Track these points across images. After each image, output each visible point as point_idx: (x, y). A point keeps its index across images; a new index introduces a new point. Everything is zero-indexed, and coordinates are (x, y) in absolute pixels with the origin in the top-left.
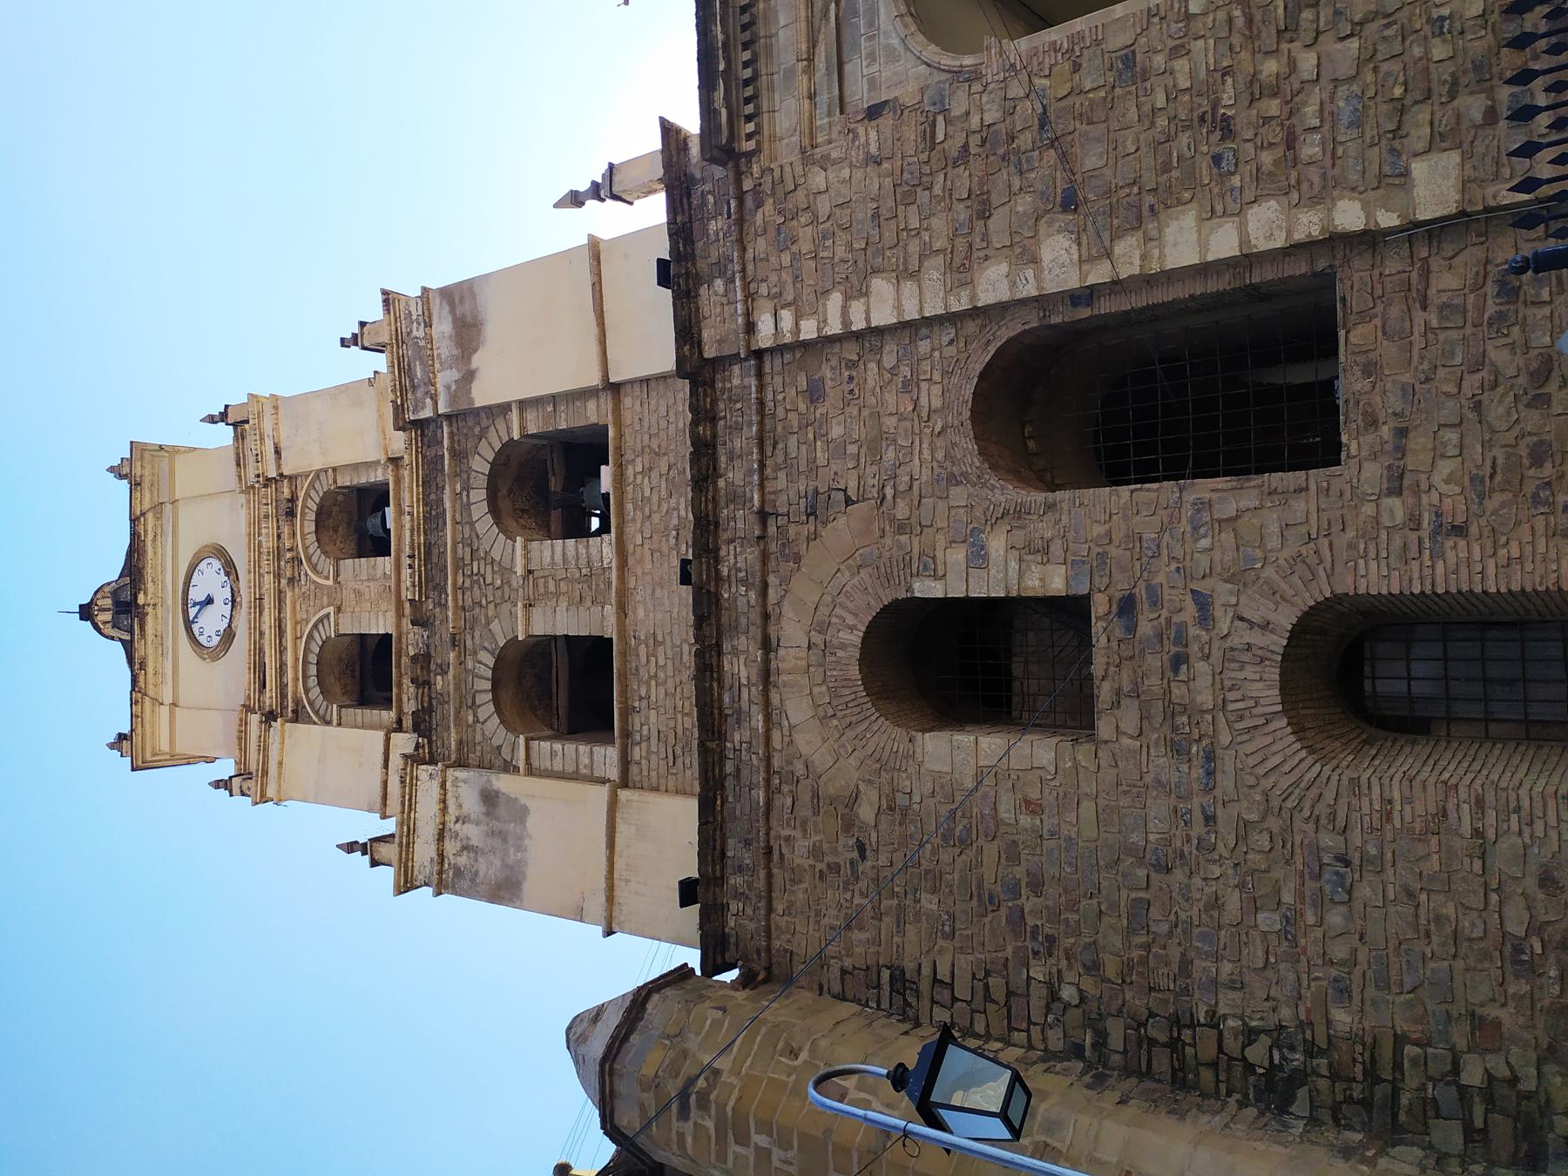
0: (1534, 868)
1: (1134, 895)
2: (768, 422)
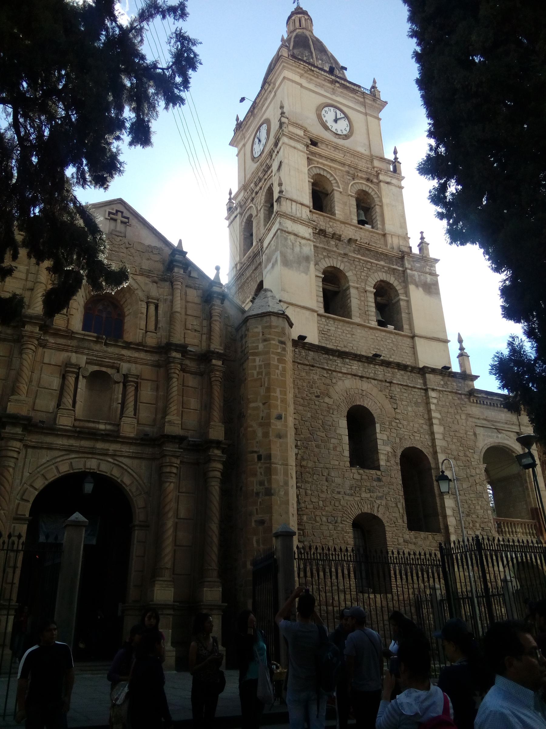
2: (410, 389)
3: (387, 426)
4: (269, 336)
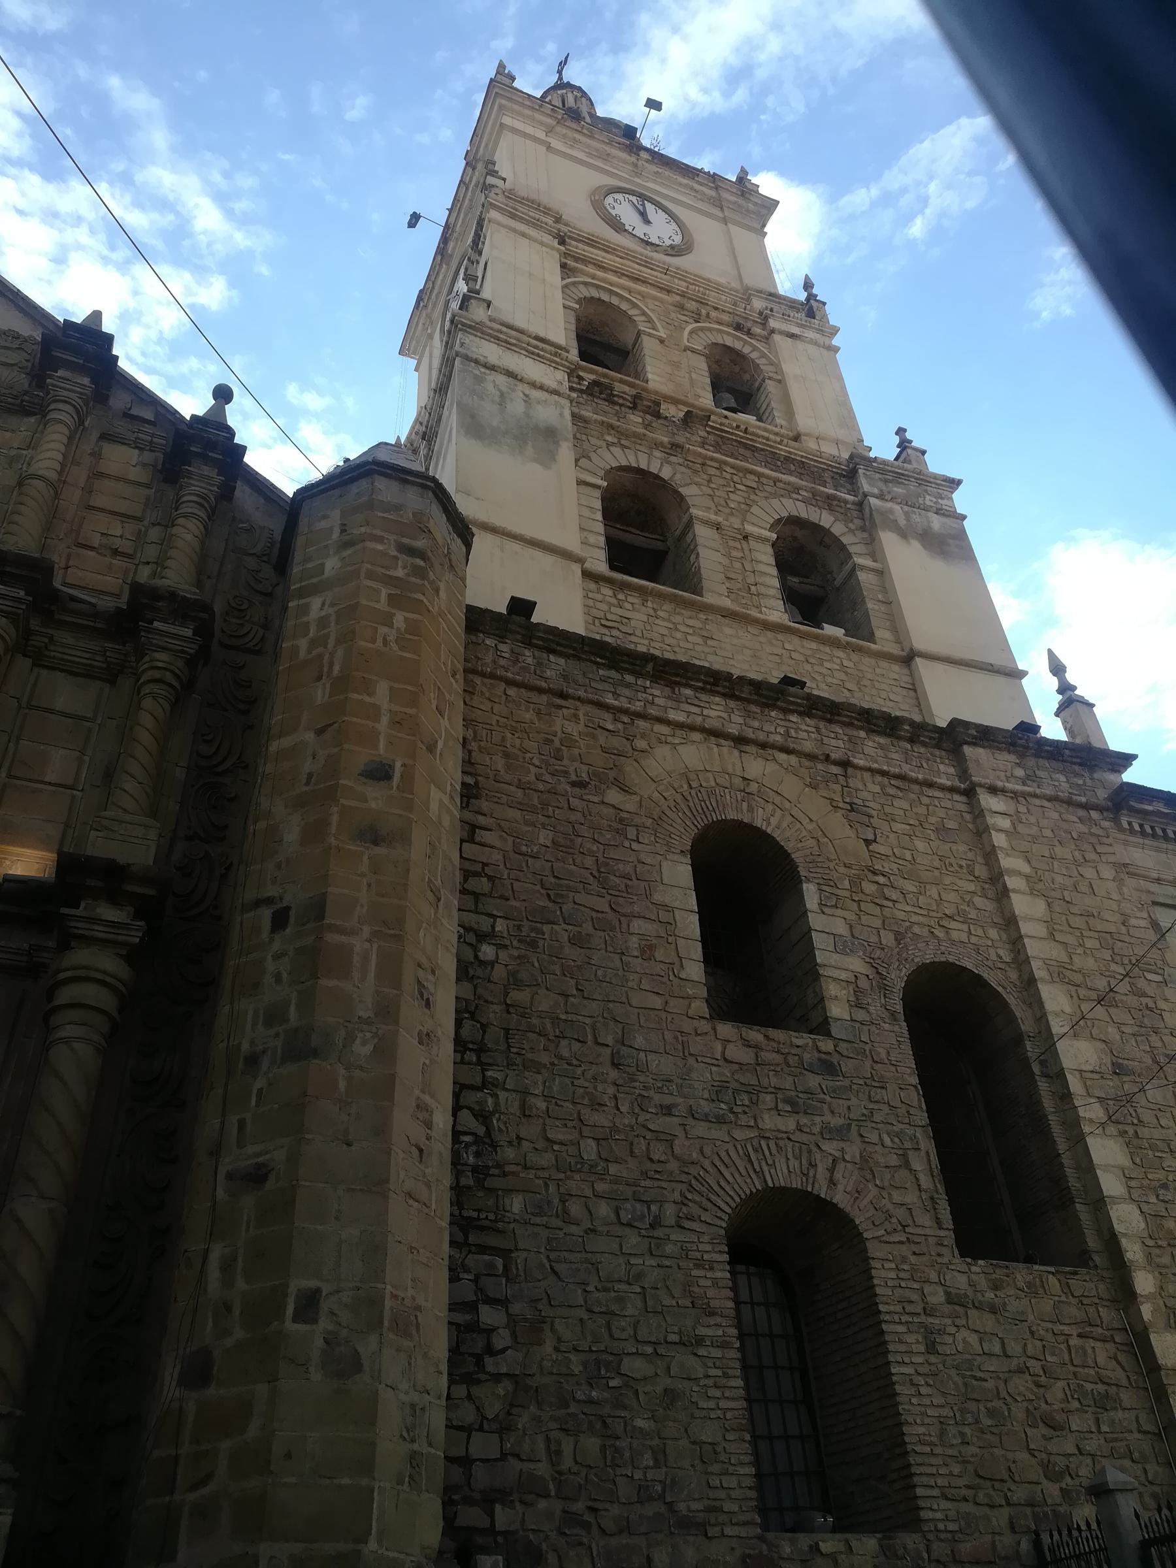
0: (680, 1386)
1: (588, 1030)
2: (916, 787)
3: (847, 894)
4: (363, 530)
